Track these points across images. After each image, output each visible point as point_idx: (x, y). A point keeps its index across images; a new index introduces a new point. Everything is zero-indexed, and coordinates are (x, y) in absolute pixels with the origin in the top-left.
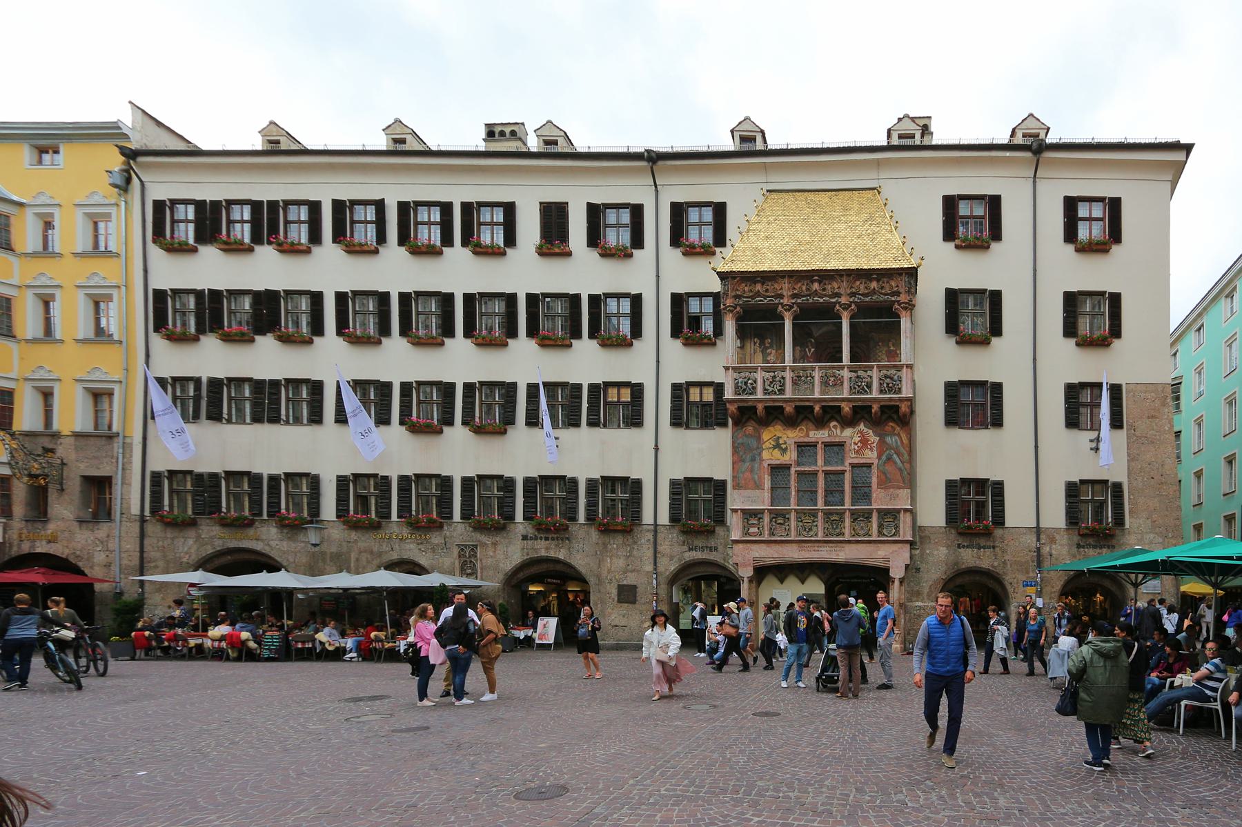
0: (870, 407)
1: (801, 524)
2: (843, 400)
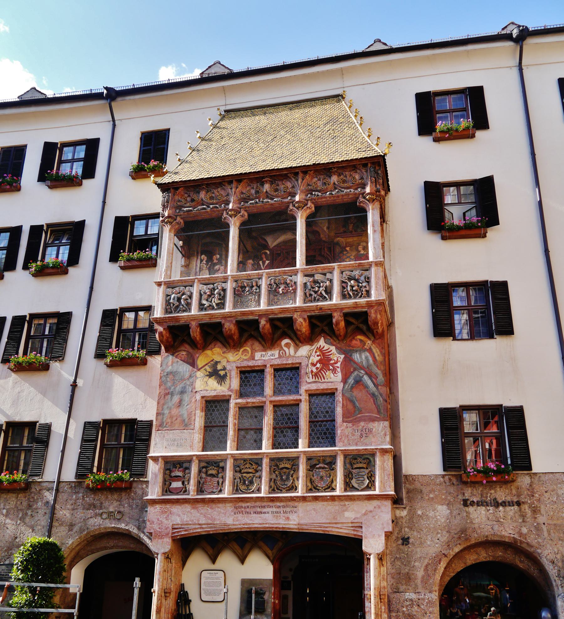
0: (330, 316)
1: (239, 475)
2: (296, 310)
